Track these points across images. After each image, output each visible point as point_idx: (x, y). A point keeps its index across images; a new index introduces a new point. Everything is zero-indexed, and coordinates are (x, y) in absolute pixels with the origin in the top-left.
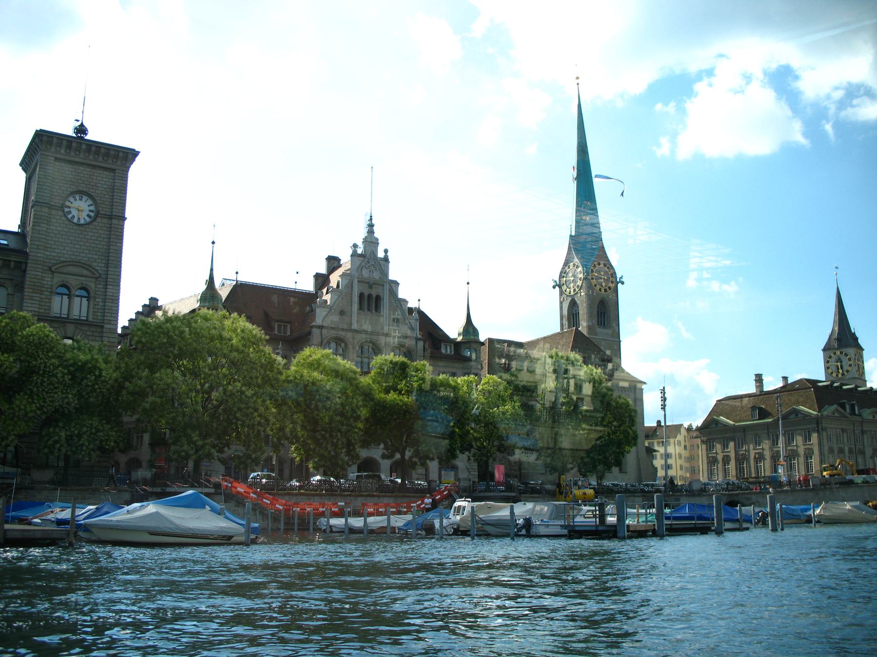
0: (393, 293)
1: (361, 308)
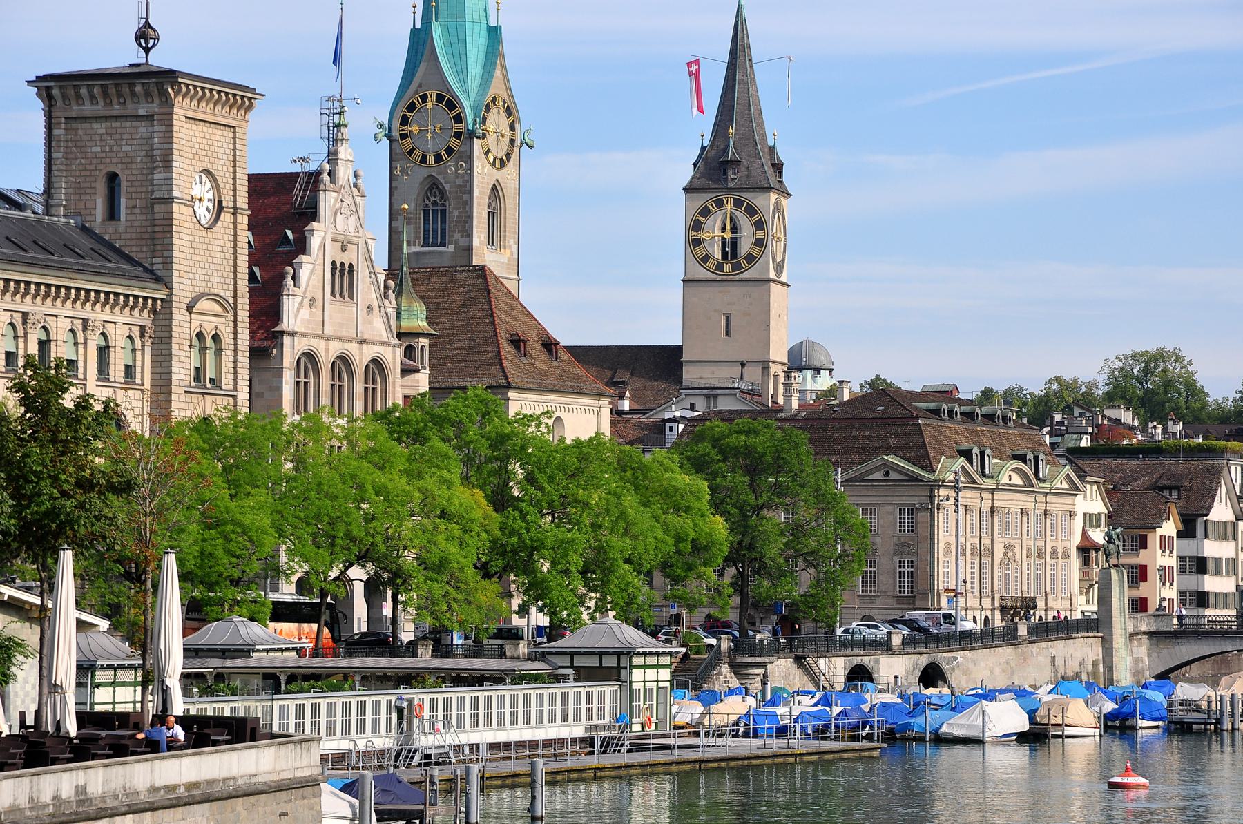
1: (333, 294)
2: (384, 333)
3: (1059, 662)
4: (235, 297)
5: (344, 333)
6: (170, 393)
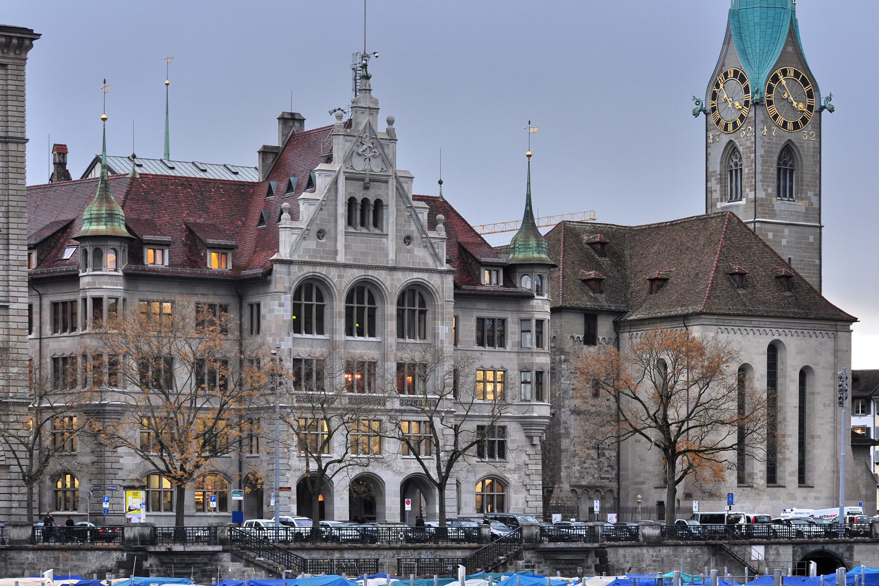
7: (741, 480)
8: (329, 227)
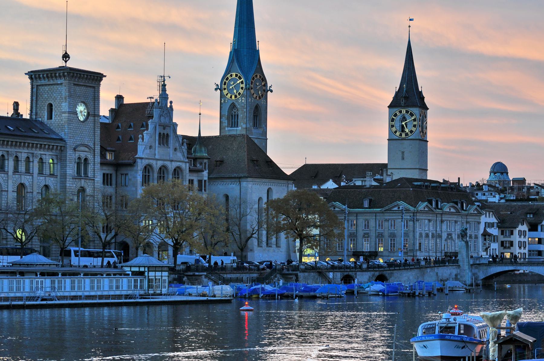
0: (175, 131)
1: (159, 144)
2: (182, 158)
3: (440, 274)
4: (94, 145)
5: (164, 158)
6: (66, 178)
7: (267, 244)
8: (153, 145)
